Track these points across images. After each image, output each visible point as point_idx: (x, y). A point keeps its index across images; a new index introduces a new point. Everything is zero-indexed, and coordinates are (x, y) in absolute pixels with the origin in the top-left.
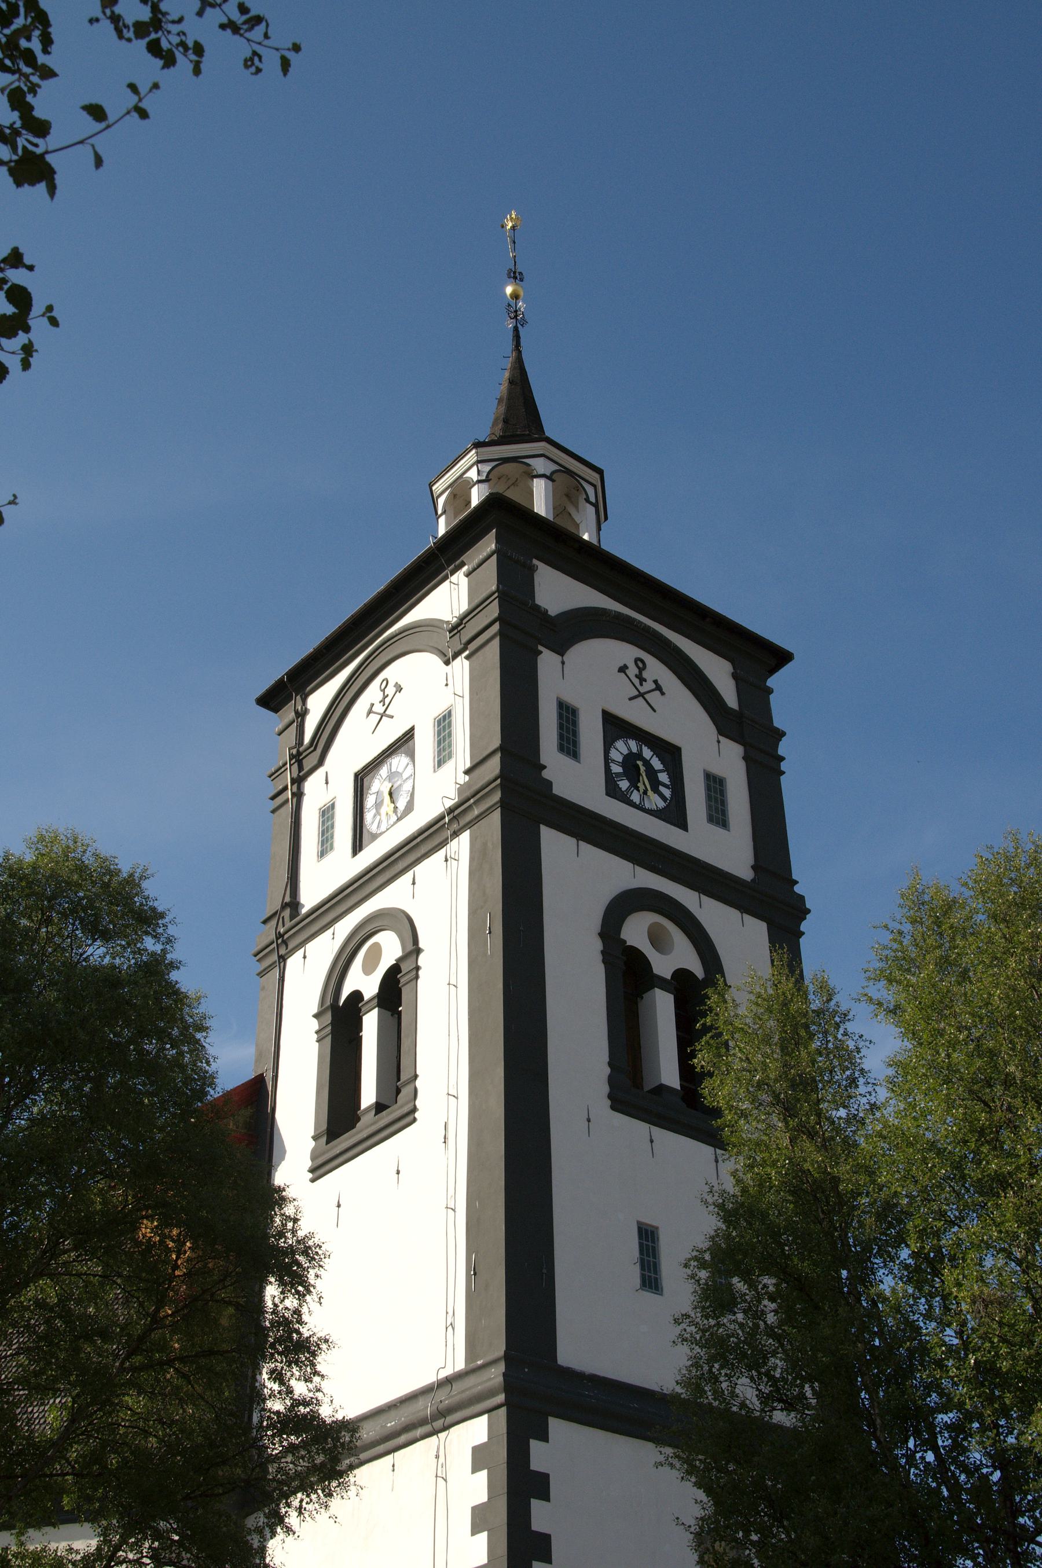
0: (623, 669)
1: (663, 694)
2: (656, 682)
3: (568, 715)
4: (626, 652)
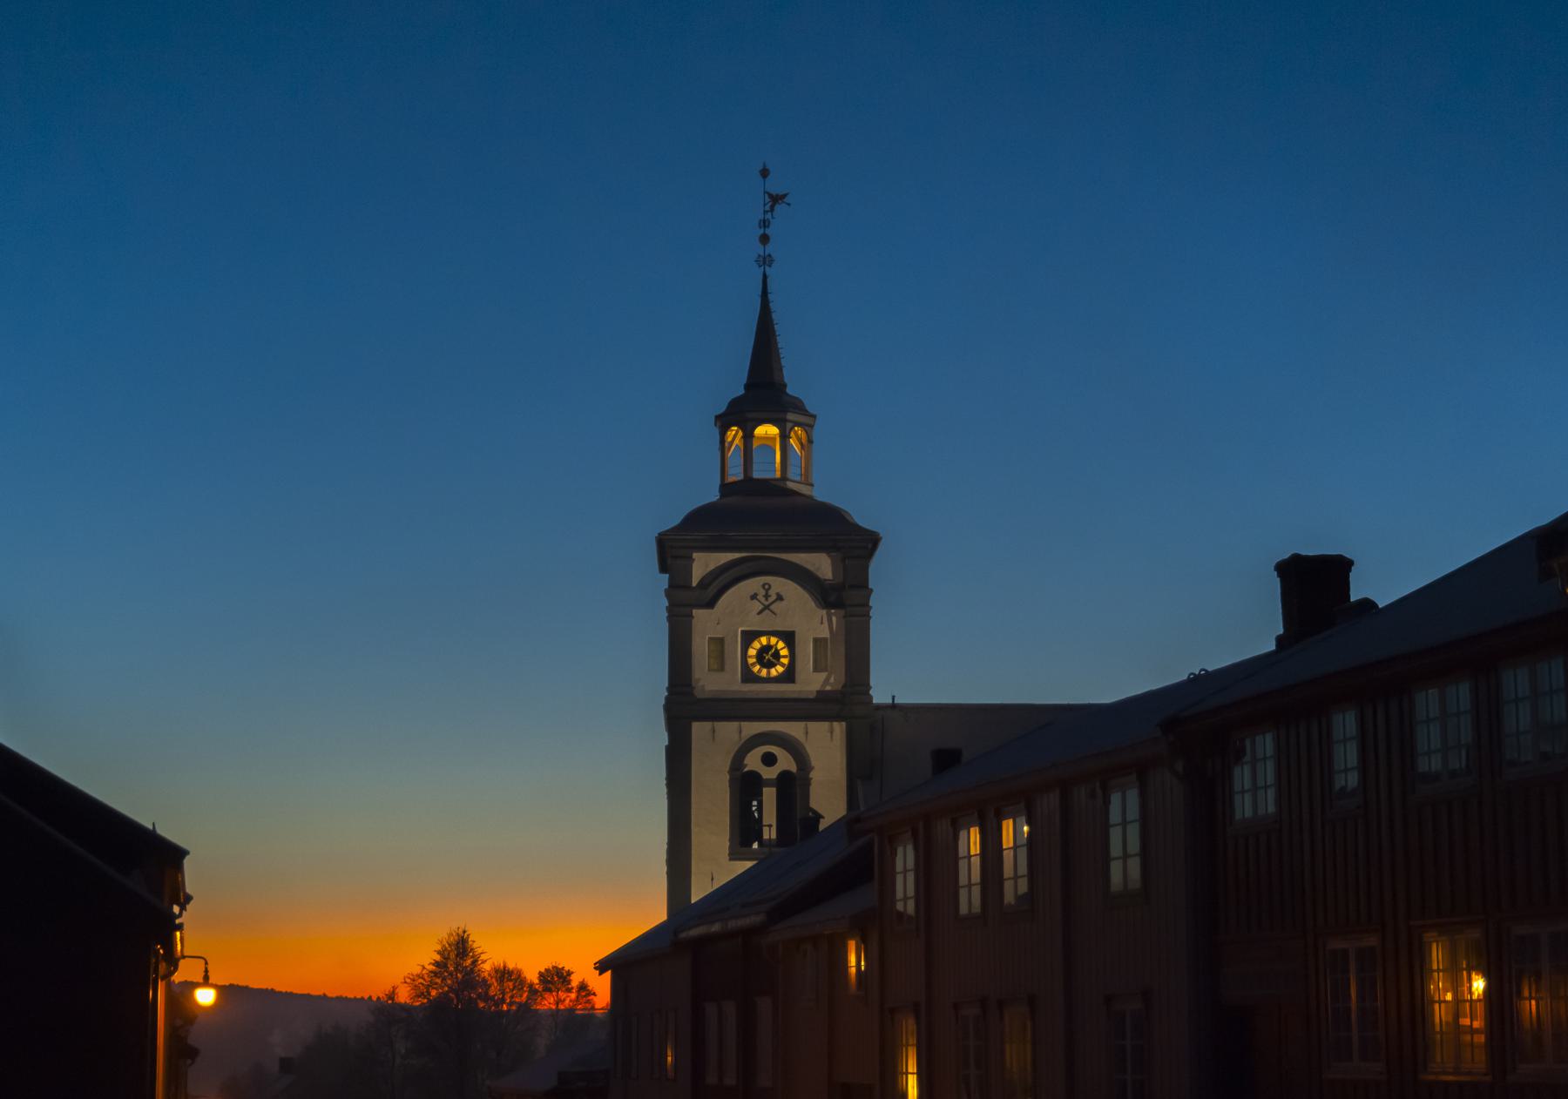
0: (754, 597)
4: (754, 584)
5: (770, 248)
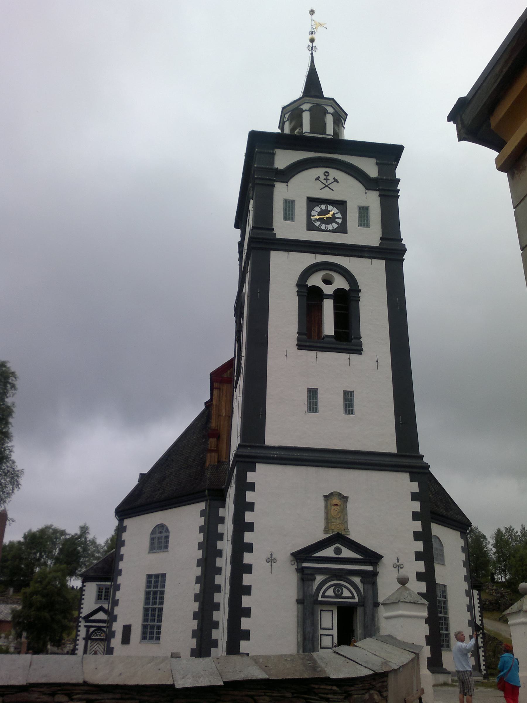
0: (318, 179)
1: (338, 182)
2: (334, 178)
3: (289, 205)
4: (319, 172)
5: (314, 44)
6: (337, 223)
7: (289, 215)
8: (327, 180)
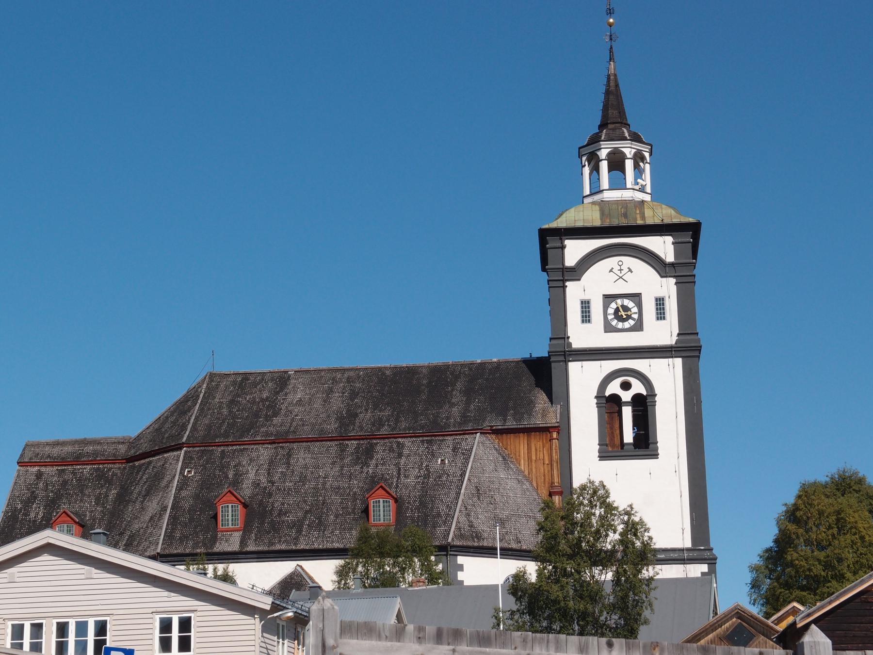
0: (611, 271)
3: (585, 306)
4: (611, 262)
6: (634, 319)
7: (586, 317)
8: (621, 270)
